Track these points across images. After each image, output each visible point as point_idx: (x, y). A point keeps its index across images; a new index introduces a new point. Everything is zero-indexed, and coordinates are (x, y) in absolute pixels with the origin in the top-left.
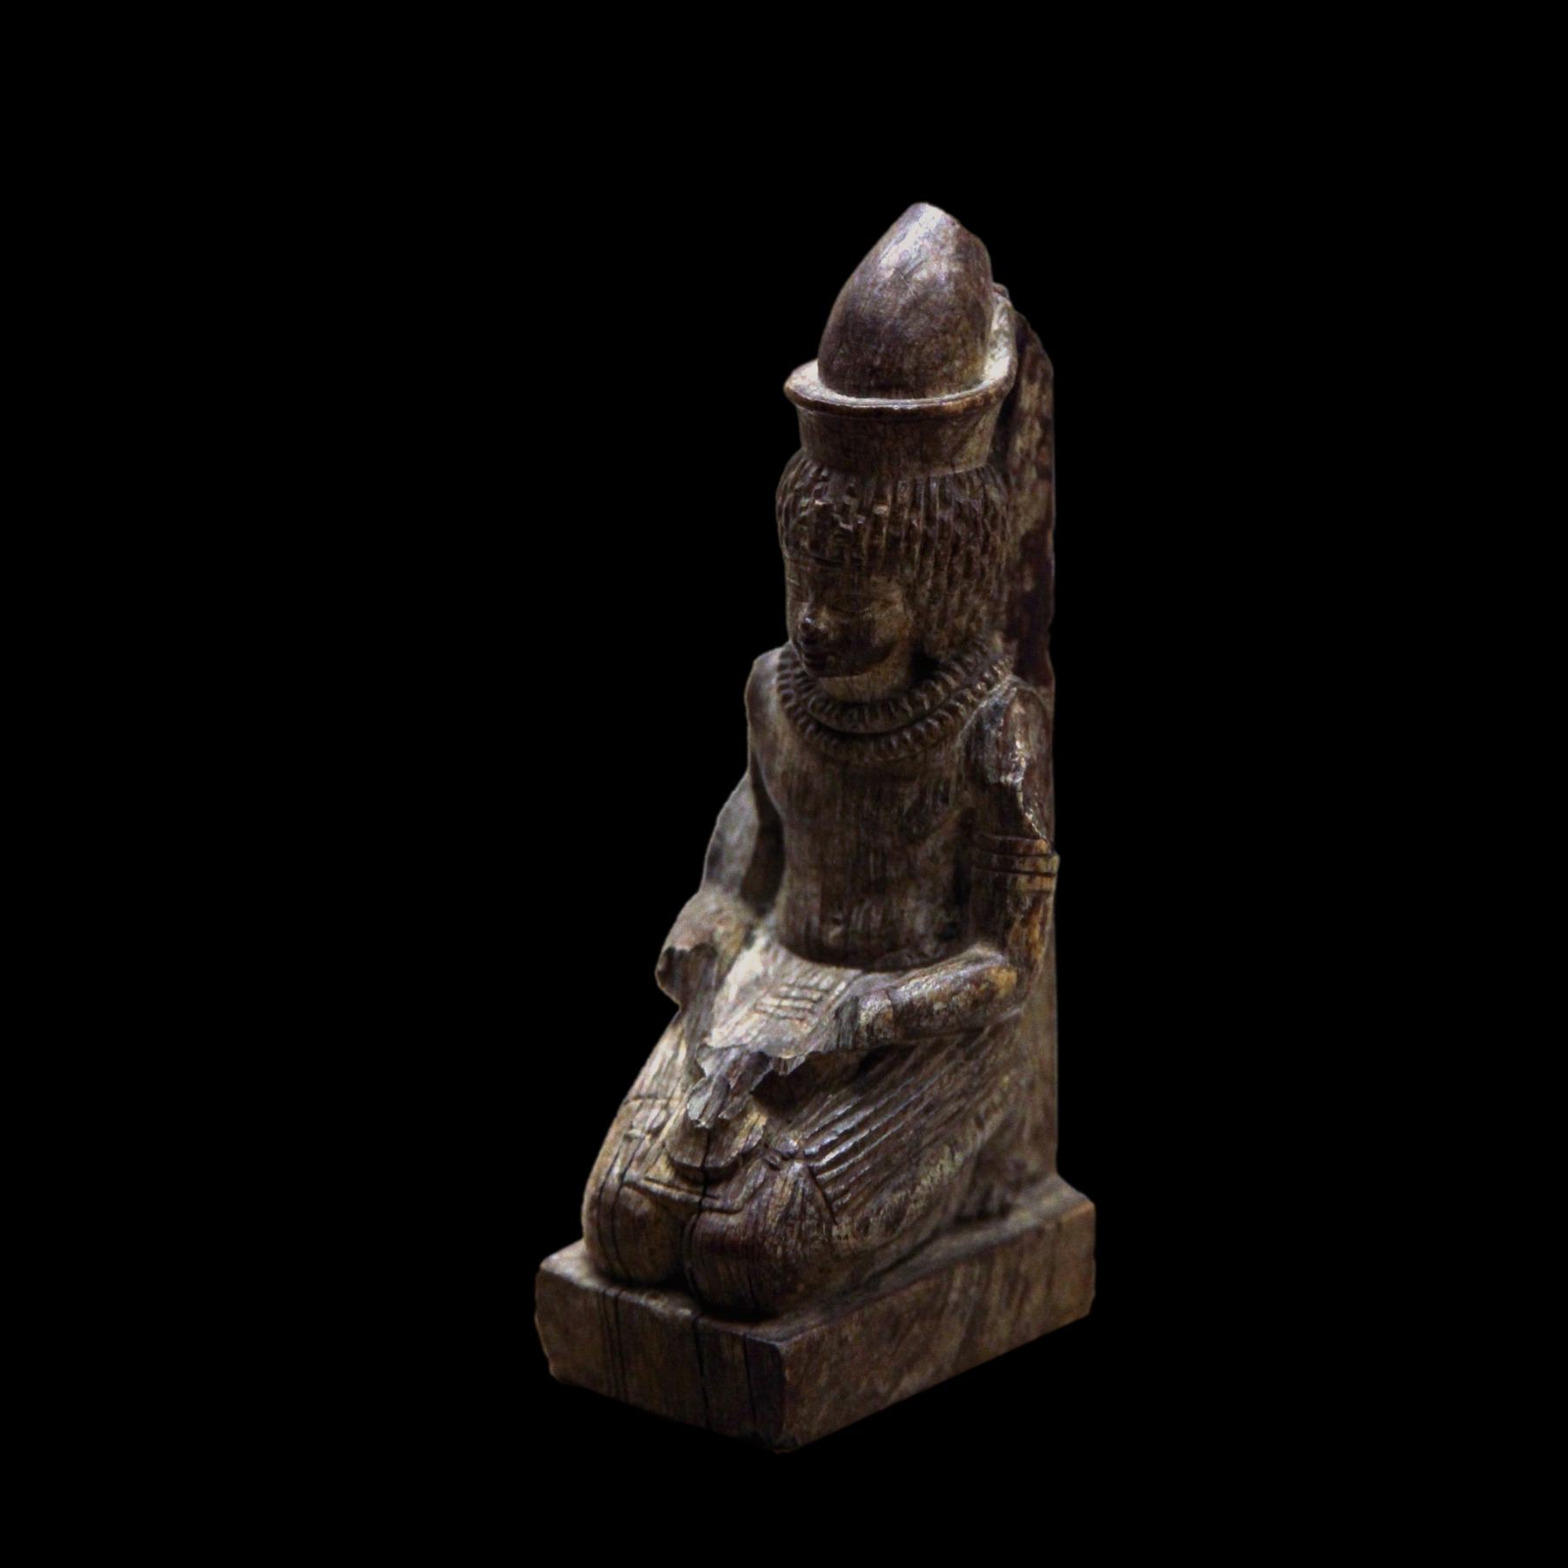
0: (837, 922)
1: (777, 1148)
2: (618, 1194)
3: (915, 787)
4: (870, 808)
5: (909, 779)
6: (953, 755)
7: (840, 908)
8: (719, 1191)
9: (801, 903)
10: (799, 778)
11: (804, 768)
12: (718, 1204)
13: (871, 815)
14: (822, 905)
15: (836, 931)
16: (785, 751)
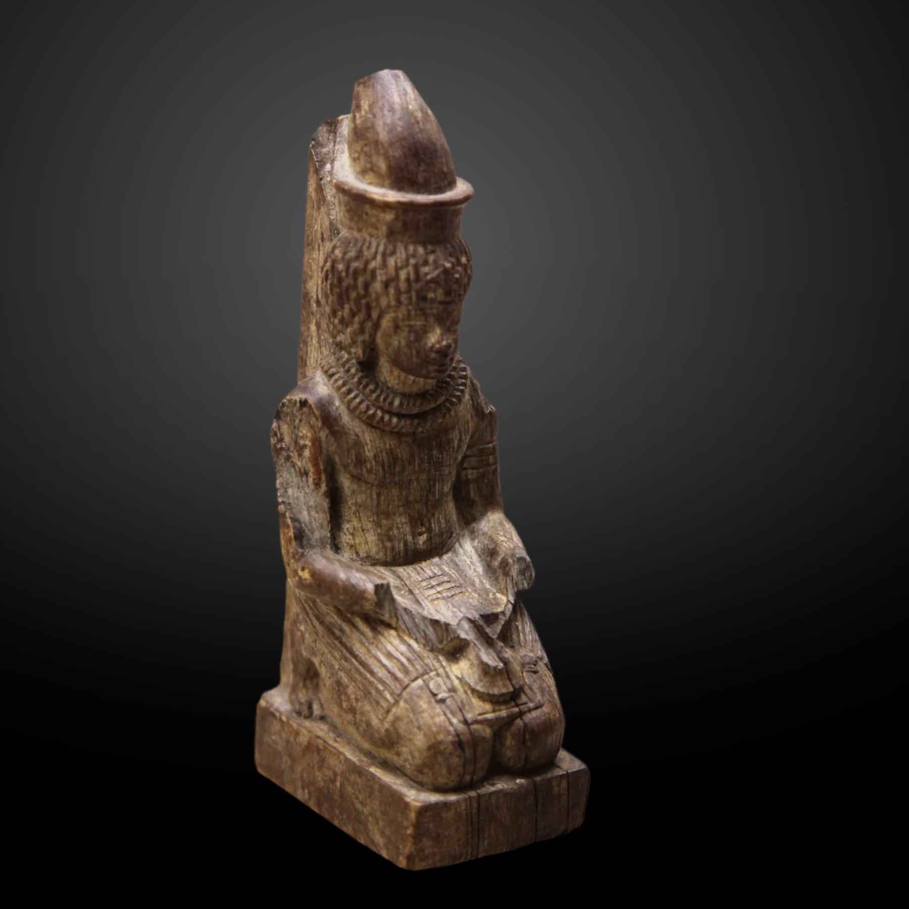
0: (420, 534)
1: (526, 661)
2: (471, 734)
3: (457, 431)
4: (437, 454)
5: (453, 428)
6: (467, 405)
7: (422, 525)
8: (524, 698)
9: (395, 531)
10: (387, 453)
11: (388, 446)
12: (531, 705)
13: (439, 458)
14: (411, 527)
15: (423, 539)
16: (368, 441)
